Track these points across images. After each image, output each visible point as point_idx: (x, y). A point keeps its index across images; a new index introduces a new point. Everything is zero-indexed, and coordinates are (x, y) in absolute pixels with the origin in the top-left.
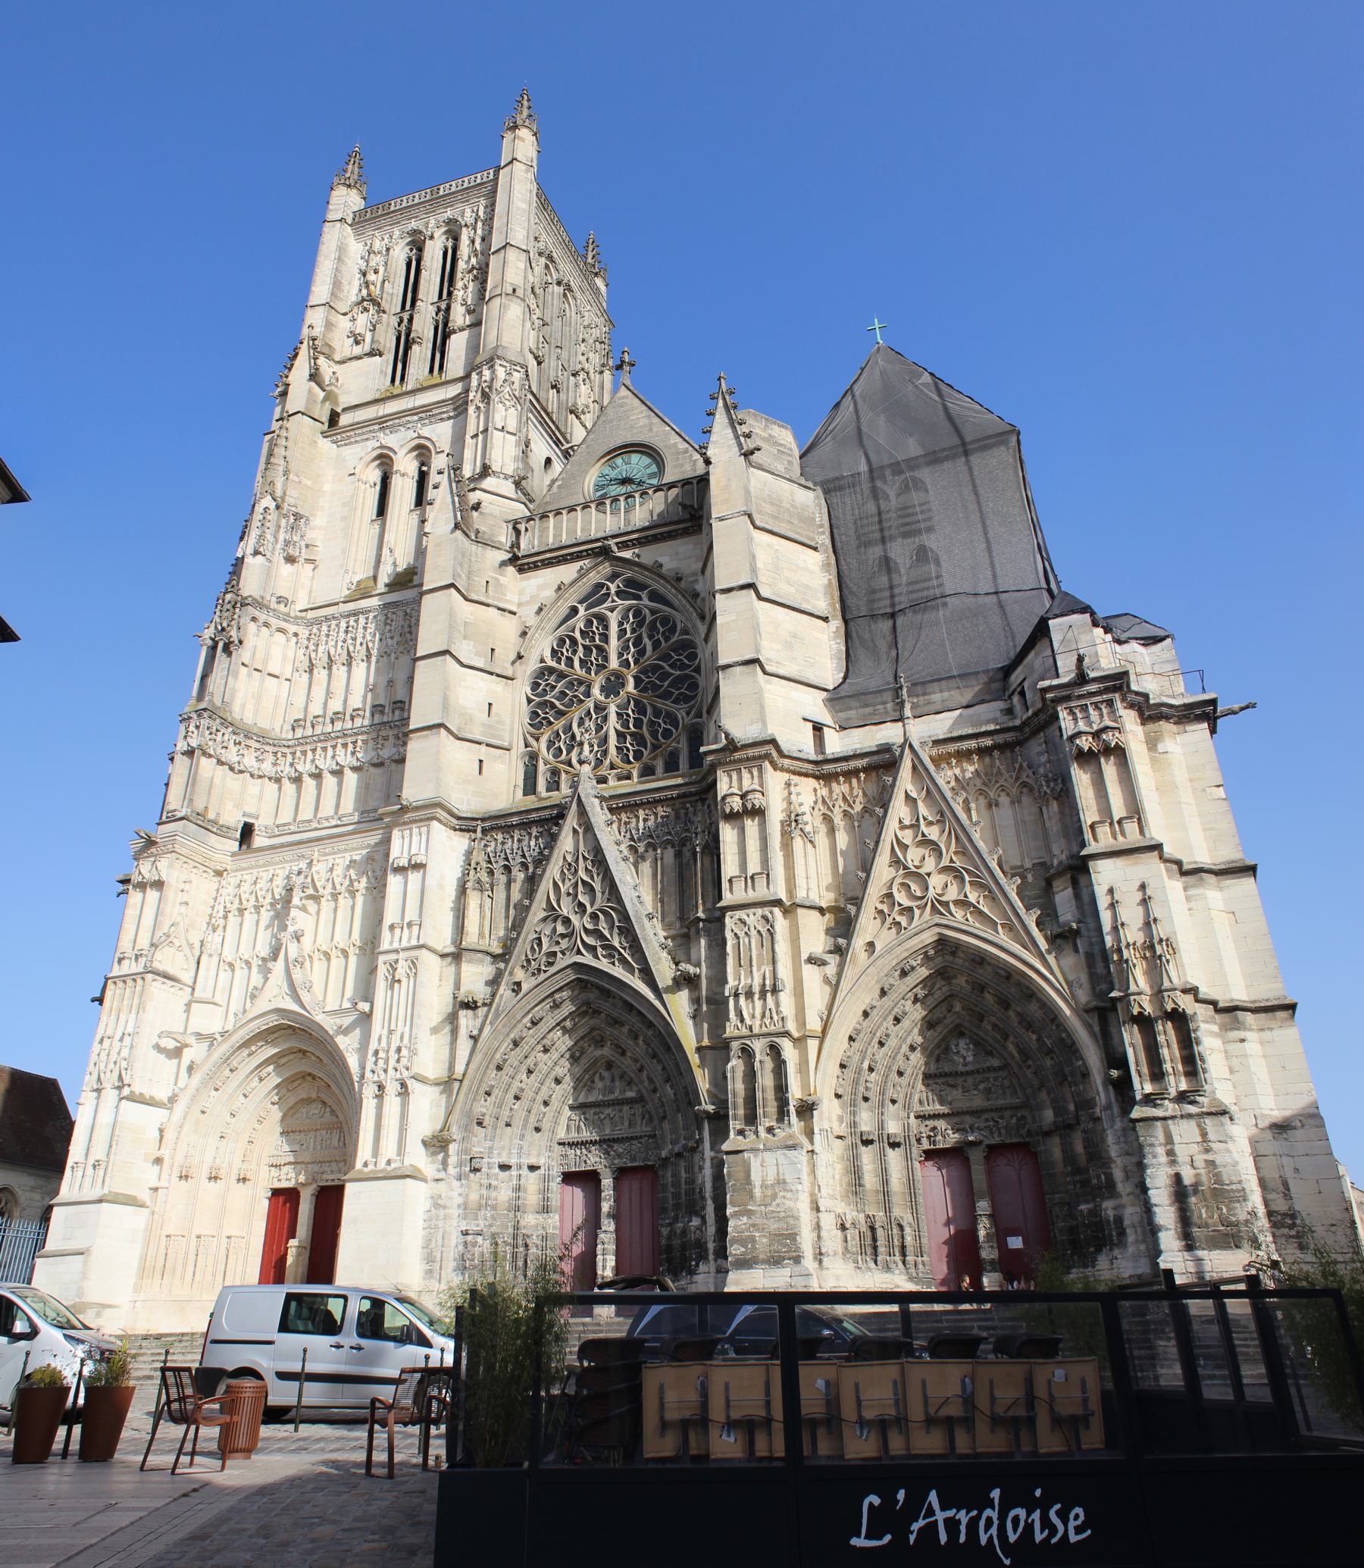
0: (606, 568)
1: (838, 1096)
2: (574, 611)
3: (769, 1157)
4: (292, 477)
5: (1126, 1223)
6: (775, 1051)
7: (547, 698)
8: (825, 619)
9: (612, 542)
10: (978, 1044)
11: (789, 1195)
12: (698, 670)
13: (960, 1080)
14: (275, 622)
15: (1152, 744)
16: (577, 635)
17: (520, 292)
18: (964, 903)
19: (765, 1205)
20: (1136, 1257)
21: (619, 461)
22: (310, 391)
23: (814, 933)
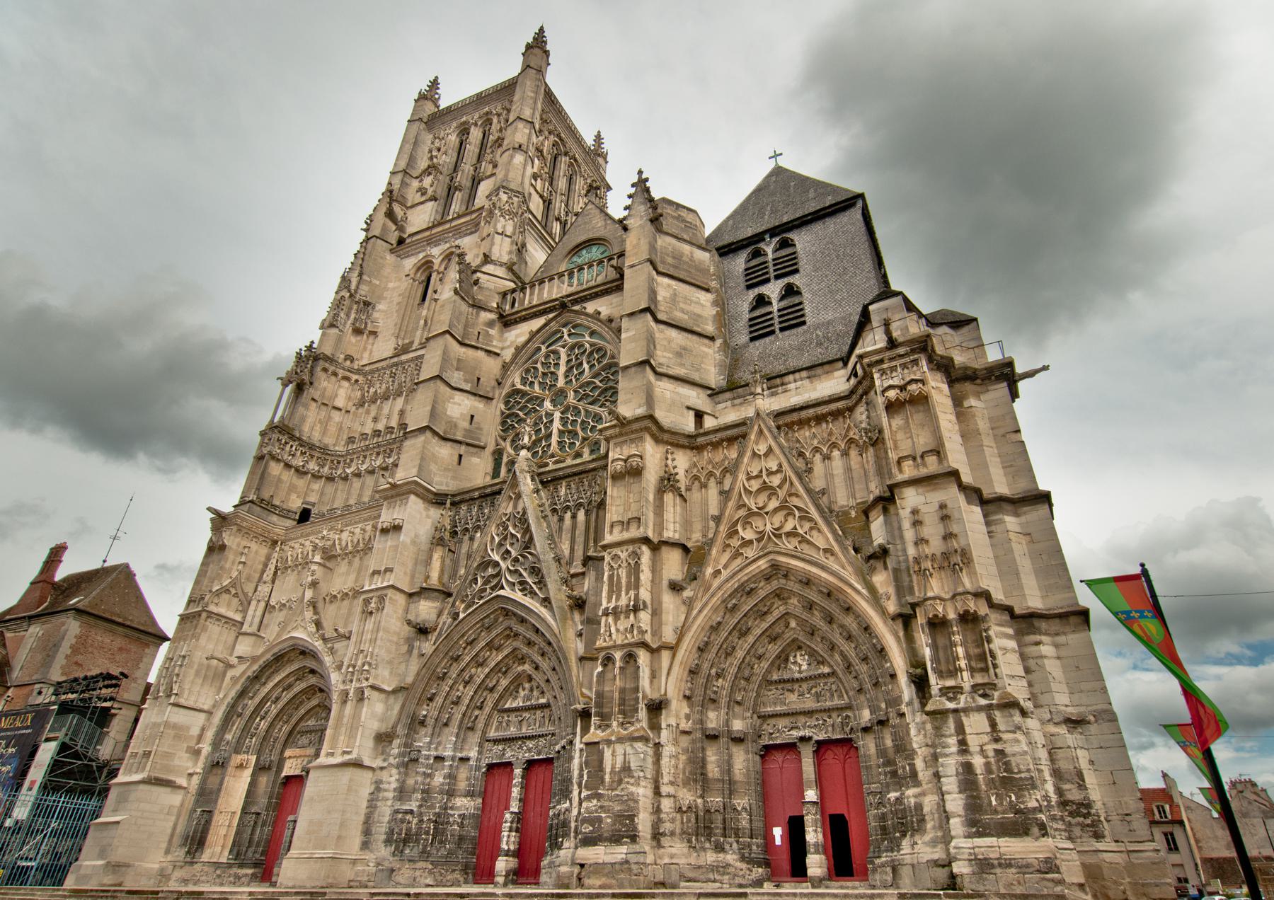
1: (687, 698)
2: (539, 349)
3: (619, 749)
4: (365, 277)
5: (926, 809)
6: (630, 658)
8: (712, 339)
10: (812, 654)
11: (632, 781)
13: (796, 686)
14: (341, 373)
15: (957, 401)
16: (539, 366)
17: (524, 148)
19: (612, 790)
20: (934, 843)
21: (584, 252)
23: (673, 565)
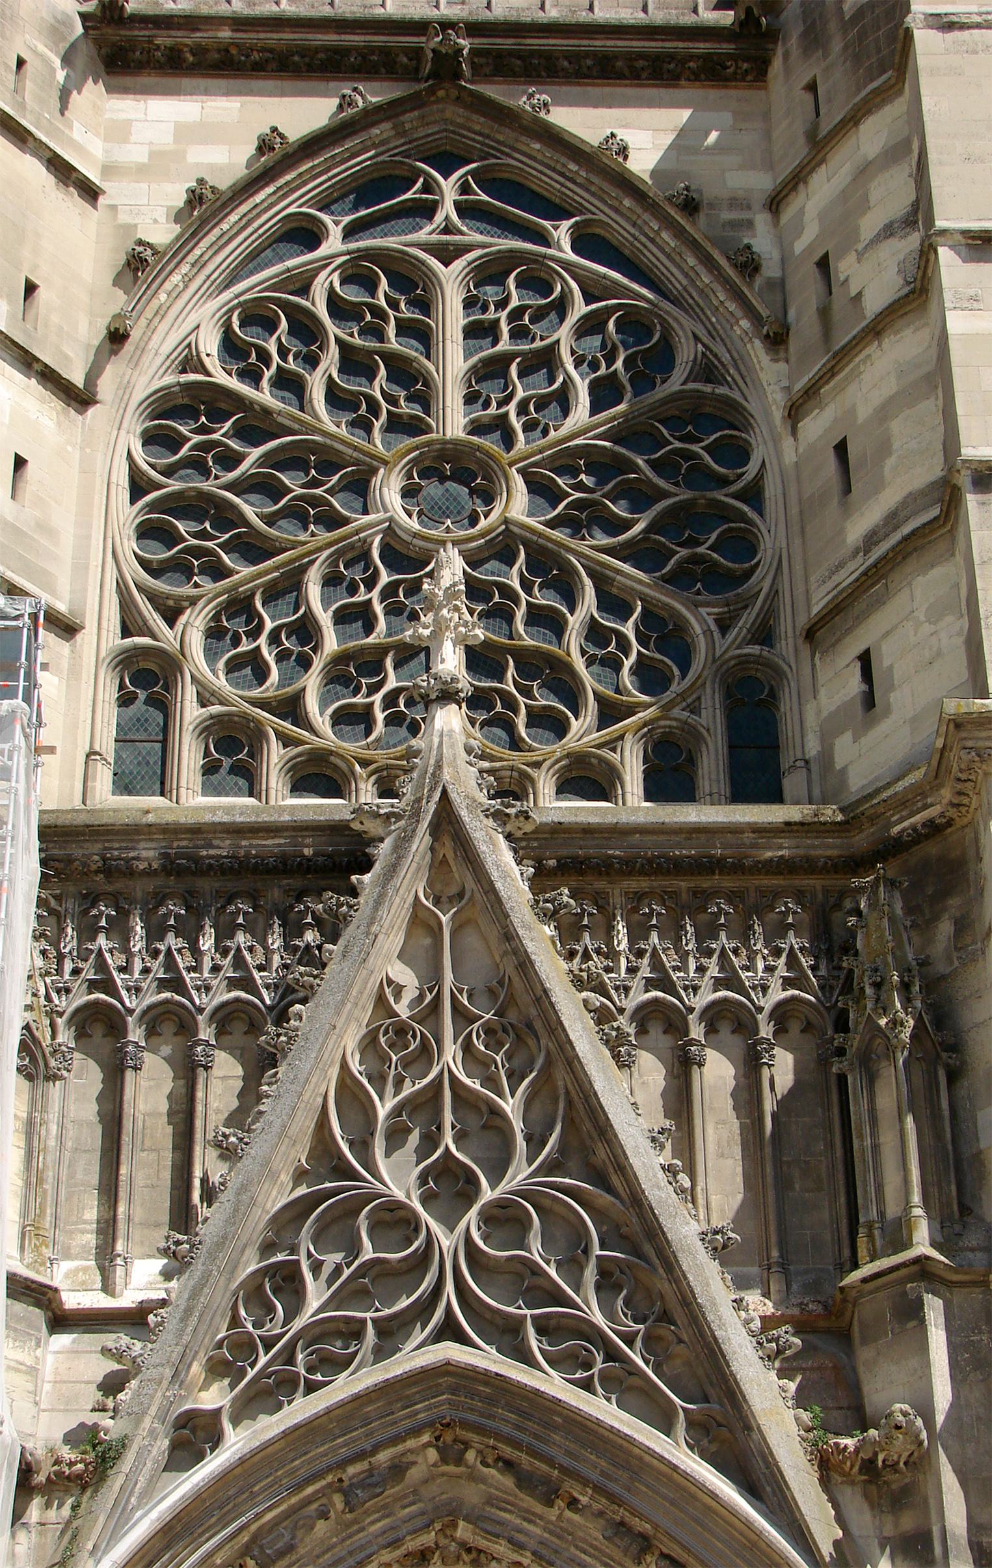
7: (207, 486)
12: (754, 494)
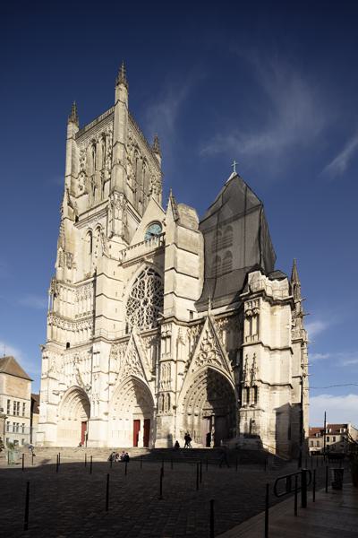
0: (144, 265)
6: (169, 395)
9: (145, 257)
18: (215, 360)
22: (69, 209)
23: (182, 367)
